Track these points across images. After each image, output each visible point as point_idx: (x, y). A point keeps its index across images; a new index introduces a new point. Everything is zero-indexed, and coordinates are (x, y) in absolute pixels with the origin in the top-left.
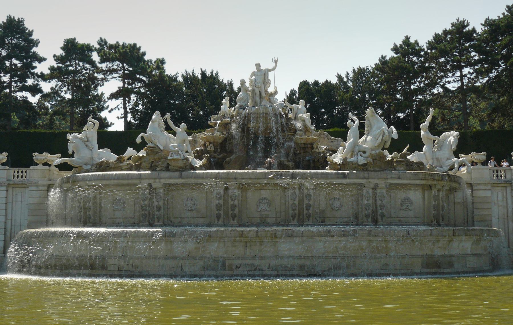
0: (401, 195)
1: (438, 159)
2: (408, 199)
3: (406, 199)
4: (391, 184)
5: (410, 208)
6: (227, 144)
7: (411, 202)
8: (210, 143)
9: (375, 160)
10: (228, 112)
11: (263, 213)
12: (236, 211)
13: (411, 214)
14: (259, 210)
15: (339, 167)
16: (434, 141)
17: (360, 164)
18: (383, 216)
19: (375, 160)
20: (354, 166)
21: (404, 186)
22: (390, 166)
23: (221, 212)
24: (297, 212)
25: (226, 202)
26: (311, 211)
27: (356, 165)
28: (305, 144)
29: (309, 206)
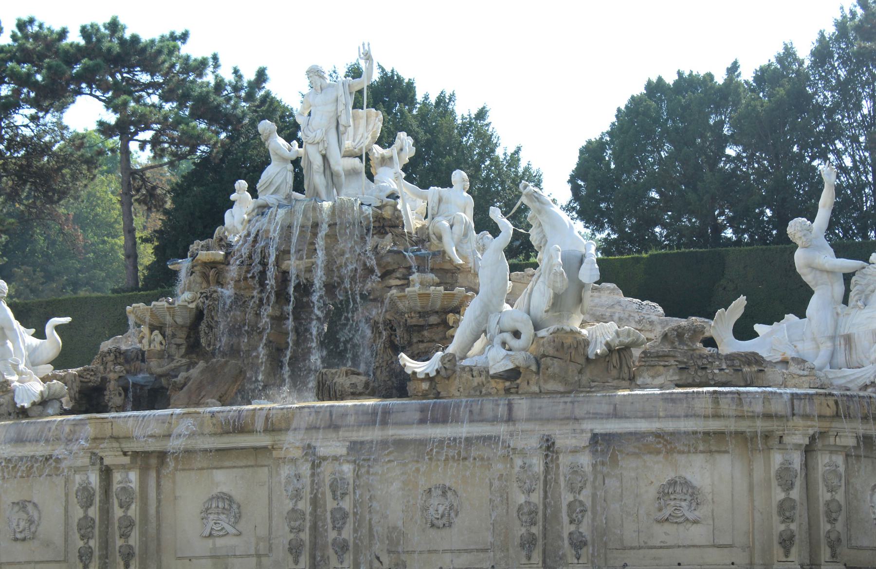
0: (658, 471)
1: (848, 340)
2: (686, 483)
3: (673, 483)
4: (595, 439)
5: (690, 516)
6: (203, 326)
7: (694, 495)
8: (152, 329)
9: (544, 356)
10: (240, 227)
11: (220, 542)
12: (134, 540)
13: (697, 534)
14: (207, 533)
15: (425, 386)
16: (848, 278)
17: (492, 372)
18: (578, 544)
19: (544, 356)
20: (477, 381)
21: (665, 443)
22: (614, 373)
23: (92, 543)
24: (305, 536)
25: (106, 512)
26: (347, 533)
27: (483, 378)
28: (423, 314)
29: (339, 517)
